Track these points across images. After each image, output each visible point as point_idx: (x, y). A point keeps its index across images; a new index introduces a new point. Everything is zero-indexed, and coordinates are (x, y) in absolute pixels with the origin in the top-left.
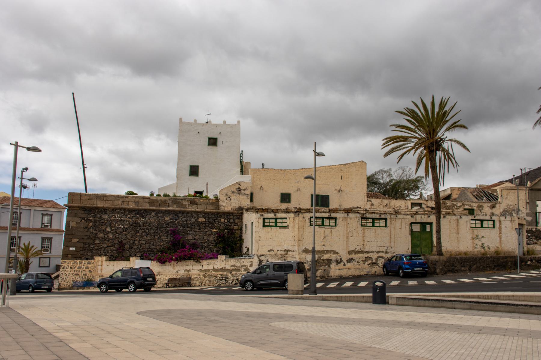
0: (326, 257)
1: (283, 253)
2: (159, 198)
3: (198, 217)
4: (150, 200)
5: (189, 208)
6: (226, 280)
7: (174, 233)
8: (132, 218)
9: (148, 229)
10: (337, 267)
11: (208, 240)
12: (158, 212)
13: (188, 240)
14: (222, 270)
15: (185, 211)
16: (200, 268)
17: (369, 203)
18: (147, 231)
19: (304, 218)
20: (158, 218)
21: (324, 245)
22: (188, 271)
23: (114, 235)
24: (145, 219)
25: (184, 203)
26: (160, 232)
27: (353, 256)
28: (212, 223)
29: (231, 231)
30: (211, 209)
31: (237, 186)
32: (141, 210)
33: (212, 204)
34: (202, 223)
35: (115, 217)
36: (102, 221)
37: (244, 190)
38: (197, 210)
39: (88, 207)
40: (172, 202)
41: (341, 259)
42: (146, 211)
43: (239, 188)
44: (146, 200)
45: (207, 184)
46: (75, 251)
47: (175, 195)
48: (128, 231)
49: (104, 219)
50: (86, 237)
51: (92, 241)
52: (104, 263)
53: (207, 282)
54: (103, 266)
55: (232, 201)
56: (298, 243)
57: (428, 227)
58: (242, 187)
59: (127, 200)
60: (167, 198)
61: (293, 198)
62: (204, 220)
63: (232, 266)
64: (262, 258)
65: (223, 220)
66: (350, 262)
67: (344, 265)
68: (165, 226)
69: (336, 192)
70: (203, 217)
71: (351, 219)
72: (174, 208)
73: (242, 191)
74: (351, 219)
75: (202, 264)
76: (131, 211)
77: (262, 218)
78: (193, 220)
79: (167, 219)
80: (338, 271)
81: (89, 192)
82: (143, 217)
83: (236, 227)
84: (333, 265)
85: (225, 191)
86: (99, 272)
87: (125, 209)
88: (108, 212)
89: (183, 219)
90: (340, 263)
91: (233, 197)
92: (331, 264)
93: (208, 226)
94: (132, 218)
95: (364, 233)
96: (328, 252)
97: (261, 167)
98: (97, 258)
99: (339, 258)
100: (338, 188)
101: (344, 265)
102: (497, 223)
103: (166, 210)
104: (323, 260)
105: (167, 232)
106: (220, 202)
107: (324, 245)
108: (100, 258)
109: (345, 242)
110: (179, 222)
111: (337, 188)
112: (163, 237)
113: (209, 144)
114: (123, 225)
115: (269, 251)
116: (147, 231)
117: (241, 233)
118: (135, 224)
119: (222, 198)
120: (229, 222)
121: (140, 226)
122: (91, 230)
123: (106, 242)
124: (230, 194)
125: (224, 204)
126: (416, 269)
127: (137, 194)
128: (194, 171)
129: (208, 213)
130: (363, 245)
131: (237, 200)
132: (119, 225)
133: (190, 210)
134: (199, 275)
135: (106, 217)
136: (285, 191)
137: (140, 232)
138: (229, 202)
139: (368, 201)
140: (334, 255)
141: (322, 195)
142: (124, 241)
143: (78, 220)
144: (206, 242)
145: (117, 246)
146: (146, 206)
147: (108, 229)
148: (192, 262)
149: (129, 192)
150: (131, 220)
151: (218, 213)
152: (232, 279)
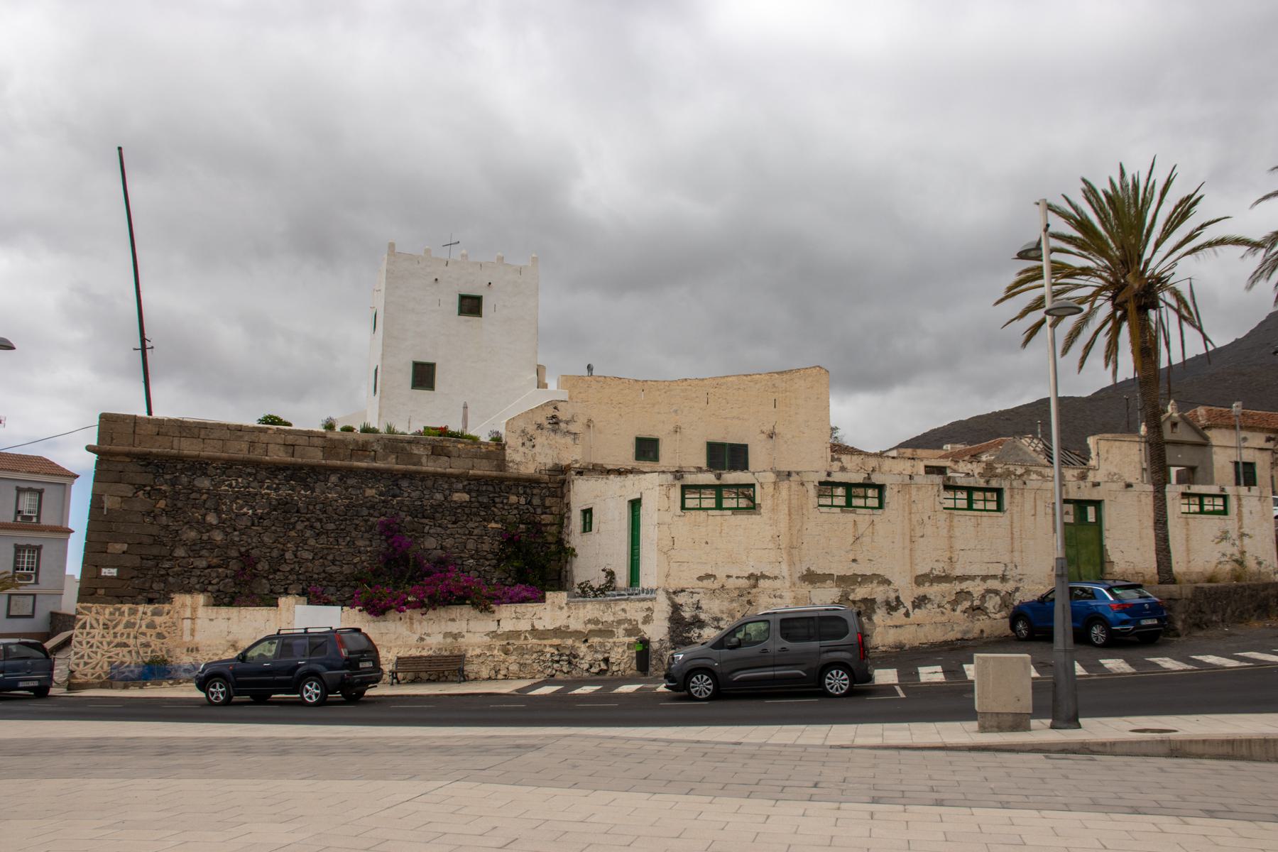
0: (860, 593)
1: (744, 583)
2: (349, 436)
3: (452, 491)
5: (430, 466)
6: (570, 663)
7: (390, 531)
8: (277, 490)
9: (320, 520)
10: (889, 622)
11: (477, 551)
13: (426, 550)
14: (557, 632)
15: (419, 473)
16: (492, 626)
17: (836, 465)
18: (318, 525)
19: (802, 484)
20: (346, 489)
21: (854, 560)
22: (456, 636)
23: (227, 534)
27: (927, 590)
28: (486, 507)
29: (537, 528)
30: (483, 469)
31: (551, 412)
32: (300, 467)
34: (461, 505)
35: (230, 486)
36: (193, 496)
37: (567, 422)
38: (449, 470)
39: (157, 456)
40: (385, 447)
41: (897, 598)
43: (553, 417)
45: (465, 407)
46: (118, 578)
47: (390, 430)
48: (266, 523)
49: (200, 491)
50: (150, 540)
51: (165, 551)
52: (202, 612)
53: (514, 668)
54: (198, 622)
55: (537, 449)
56: (790, 554)
57: (1091, 511)
58: (561, 415)
61: (664, 450)
62: (466, 497)
63: (589, 621)
64: (680, 599)
65: (513, 499)
66: (919, 607)
67: (907, 615)
69: (764, 437)
70: (464, 490)
71: (919, 489)
72: (390, 463)
73: (562, 425)
74: (919, 489)
75: (497, 616)
76: (275, 469)
77: (679, 484)
78: (439, 496)
79: (369, 492)
80: (892, 631)
81: (158, 413)
82: (307, 487)
83: (547, 519)
84: (880, 617)
85: (521, 424)
86: (187, 638)
87: (257, 464)
88: (210, 470)
89: (413, 494)
90: (895, 609)
92: (874, 612)
93: (477, 514)
94: (277, 490)
95: (951, 527)
96: (866, 579)
97: (585, 373)
98: (181, 599)
99: (892, 595)
100: (767, 428)
101: (907, 615)
102: (1233, 503)
103: (367, 470)
104: (854, 602)
105: (371, 527)
106: (508, 451)
107: (854, 560)
108: (187, 599)
109: (907, 552)
110: (402, 502)
111: (764, 429)
112: (360, 543)
113: (462, 311)
114: (252, 507)
115: (700, 579)
116: (318, 525)
117: (560, 532)
118: (285, 506)
119: (511, 440)
120: (529, 503)
122: (164, 520)
123: (204, 552)
125: (517, 458)
126: (1144, 622)
127: (290, 425)
128: (424, 376)
129: (477, 479)
130: (950, 559)
131: (550, 446)
132: (242, 507)
133: (431, 469)
134: (490, 648)
135: (205, 483)
136: (646, 433)
137: (300, 526)
139: (833, 459)
140: (881, 588)
141: (731, 445)
142: (255, 553)
143: (128, 490)
144: (472, 557)
145: (234, 565)
146: (316, 457)
147: (212, 519)
148: (466, 611)
149: (270, 417)
150: (273, 495)
151: (502, 480)
152: (589, 658)
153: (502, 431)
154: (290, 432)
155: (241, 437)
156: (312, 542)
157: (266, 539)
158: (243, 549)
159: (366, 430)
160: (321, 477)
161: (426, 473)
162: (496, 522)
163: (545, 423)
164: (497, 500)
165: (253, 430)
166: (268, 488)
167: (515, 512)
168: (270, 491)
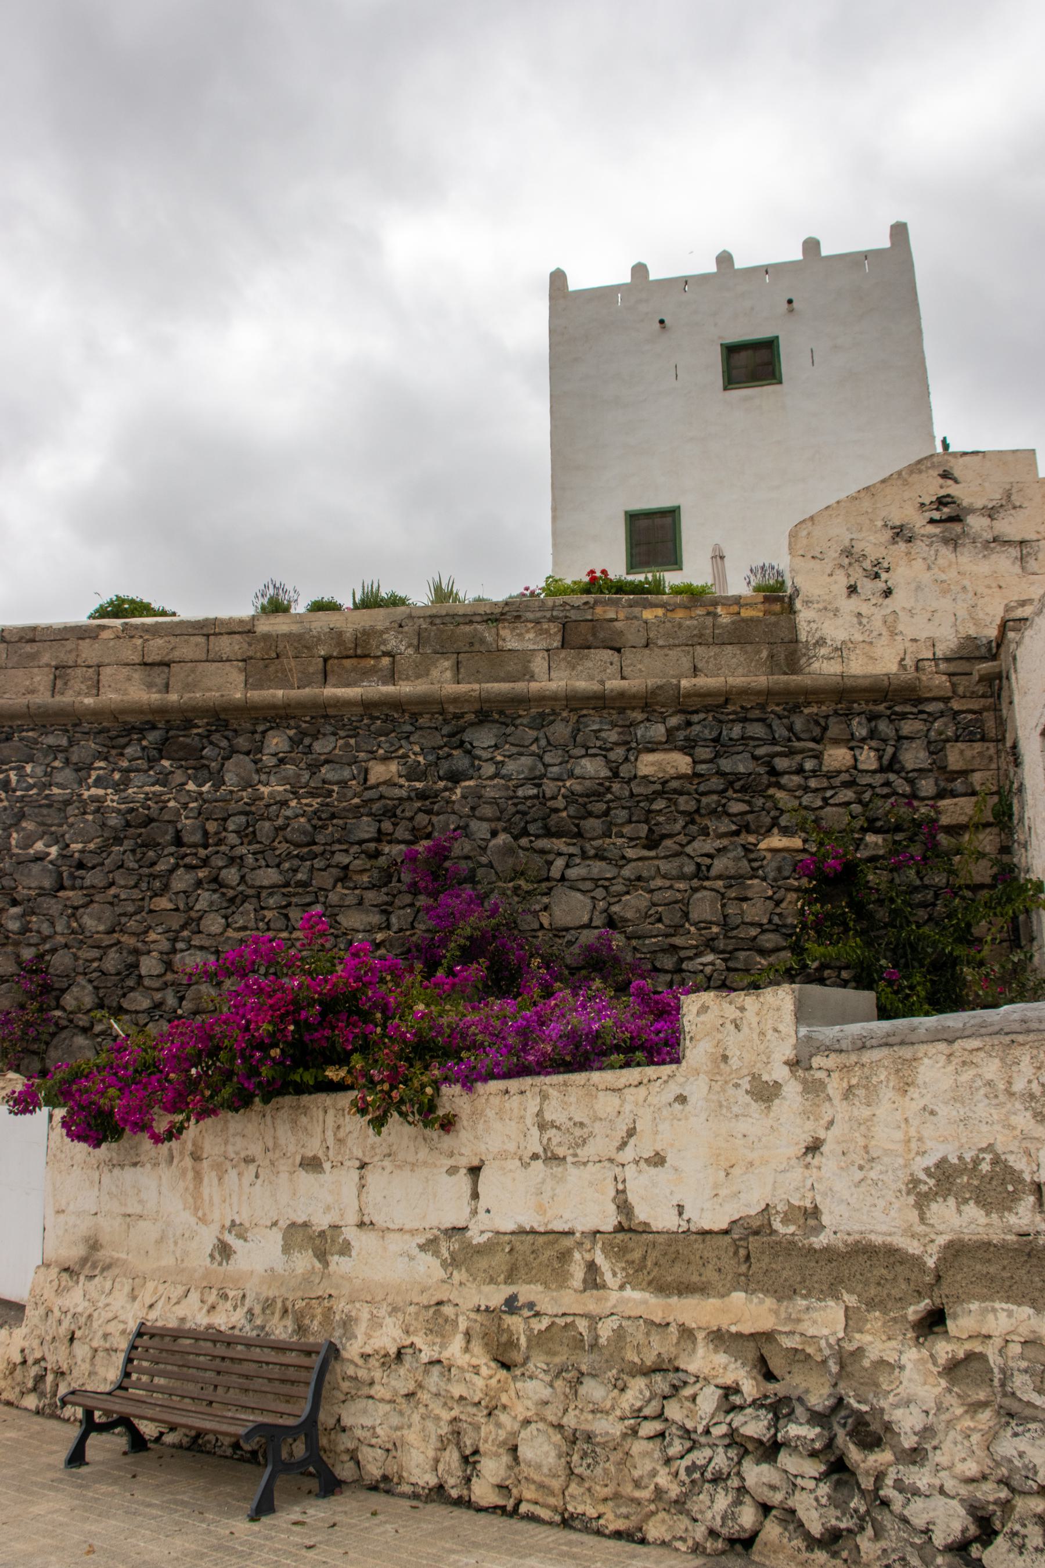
2: (323, 621)
3: (635, 748)
4: (263, 642)
5: (555, 678)
7: (437, 873)
8: (119, 787)
11: (725, 923)
12: (308, 722)
13: (559, 932)
14: (760, 1250)
20: (314, 768)
24: (219, 783)
25: (512, 644)
26: (323, 879)
28: (747, 787)
29: (923, 841)
30: (732, 672)
31: (931, 487)
33: (740, 635)
34: (665, 789)
37: (991, 512)
38: (614, 684)
40: (420, 640)
42: (222, 720)
43: (942, 502)
44: (226, 645)
48: (92, 878)
53: (540, 1450)
55: (900, 599)
59: (90, 652)
60: (378, 618)
62: (681, 762)
63: (945, 1179)
65: (837, 757)
68: (366, 828)
70: (670, 743)
72: (441, 681)
73: (976, 523)
76: (120, 730)
78: (592, 767)
79: (379, 772)
82: (201, 770)
83: (955, 810)
85: (839, 532)
87: (71, 722)
89: (511, 767)
91: (907, 571)
93: (720, 812)
94: (126, 782)
103: (368, 706)
106: (804, 615)
112: (352, 920)
113: (732, 380)
114: (57, 839)
116: (231, 875)
117: (1006, 849)
118: (140, 828)
119: (816, 585)
120: (891, 766)
121: (178, 841)
124: (874, 553)
125: (836, 631)
127: (174, 614)
129: (716, 705)
131: (944, 588)
132: (28, 842)
137: (181, 881)
138: (877, 614)
142: (60, 961)
144: (709, 945)
146: (229, 686)
149: (121, 601)
150: (112, 800)
151: (794, 700)
153: (783, 562)
154: (154, 631)
155: (33, 657)
156: (214, 924)
157: (89, 922)
158: (27, 954)
160: (242, 742)
161: (542, 698)
162: (786, 831)
163: (918, 521)
164: (781, 764)
165: (80, 633)
166: (99, 782)
167: (848, 795)
168: (108, 792)
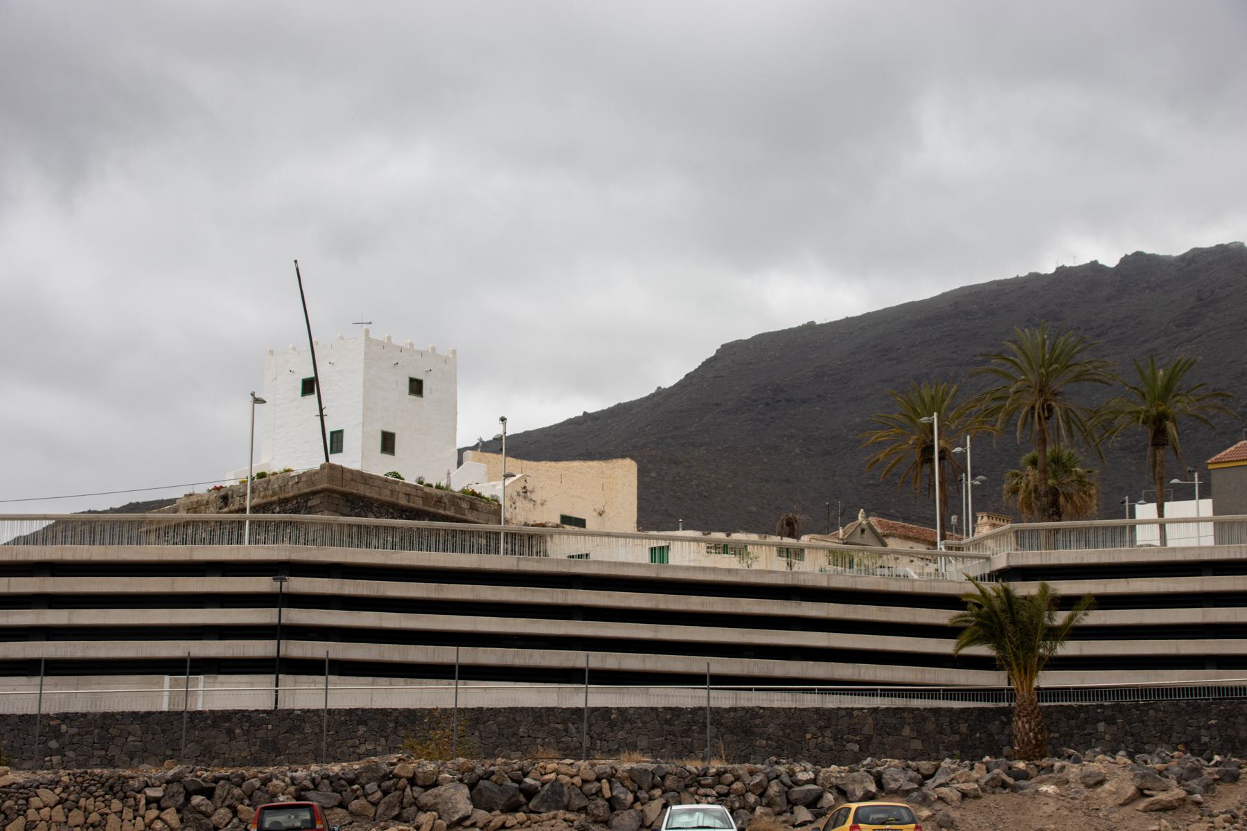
58: (529, 488)
69: (595, 514)
100: (599, 507)
128: (388, 443)
159: (438, 487)
